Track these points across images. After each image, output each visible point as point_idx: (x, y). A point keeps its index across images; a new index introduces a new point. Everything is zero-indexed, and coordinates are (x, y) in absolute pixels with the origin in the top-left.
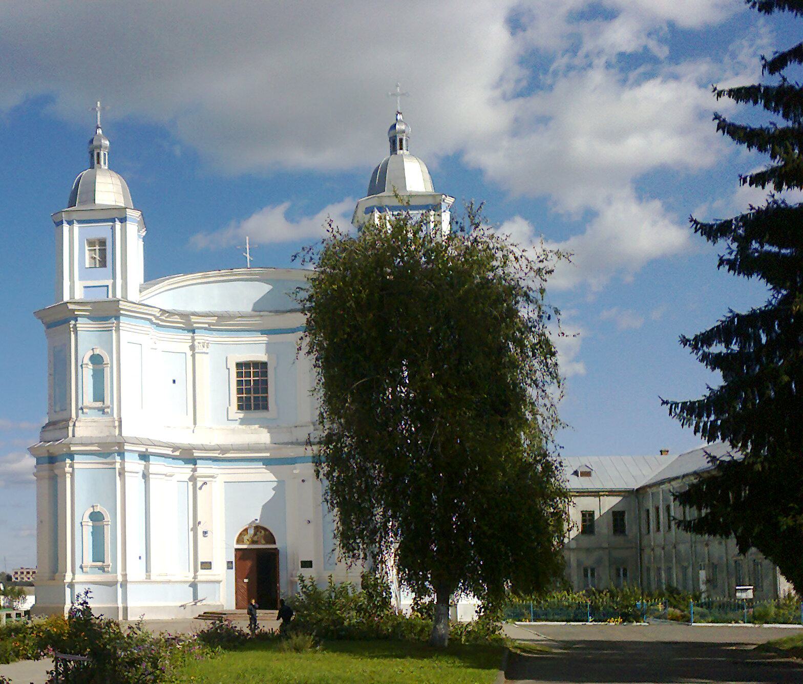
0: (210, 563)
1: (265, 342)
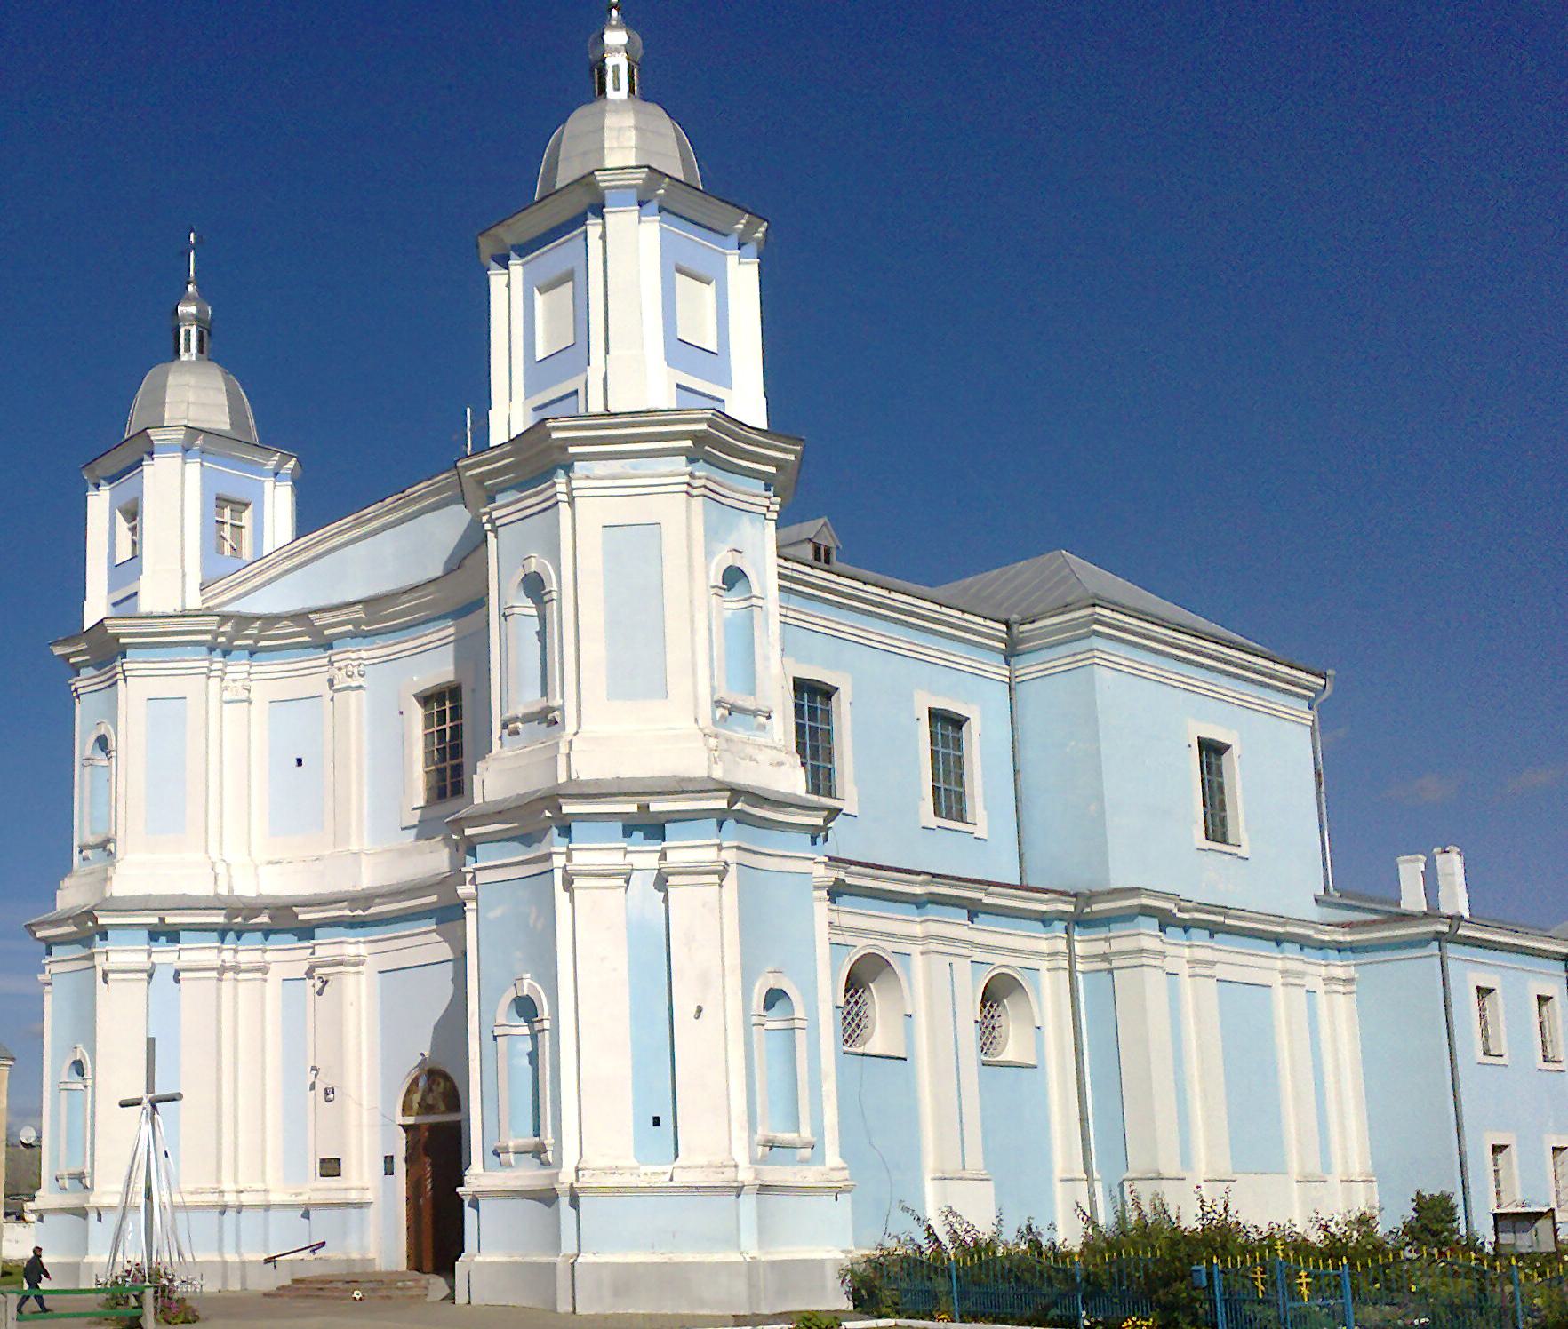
0: (339, 1160)
1: (452, 638)
